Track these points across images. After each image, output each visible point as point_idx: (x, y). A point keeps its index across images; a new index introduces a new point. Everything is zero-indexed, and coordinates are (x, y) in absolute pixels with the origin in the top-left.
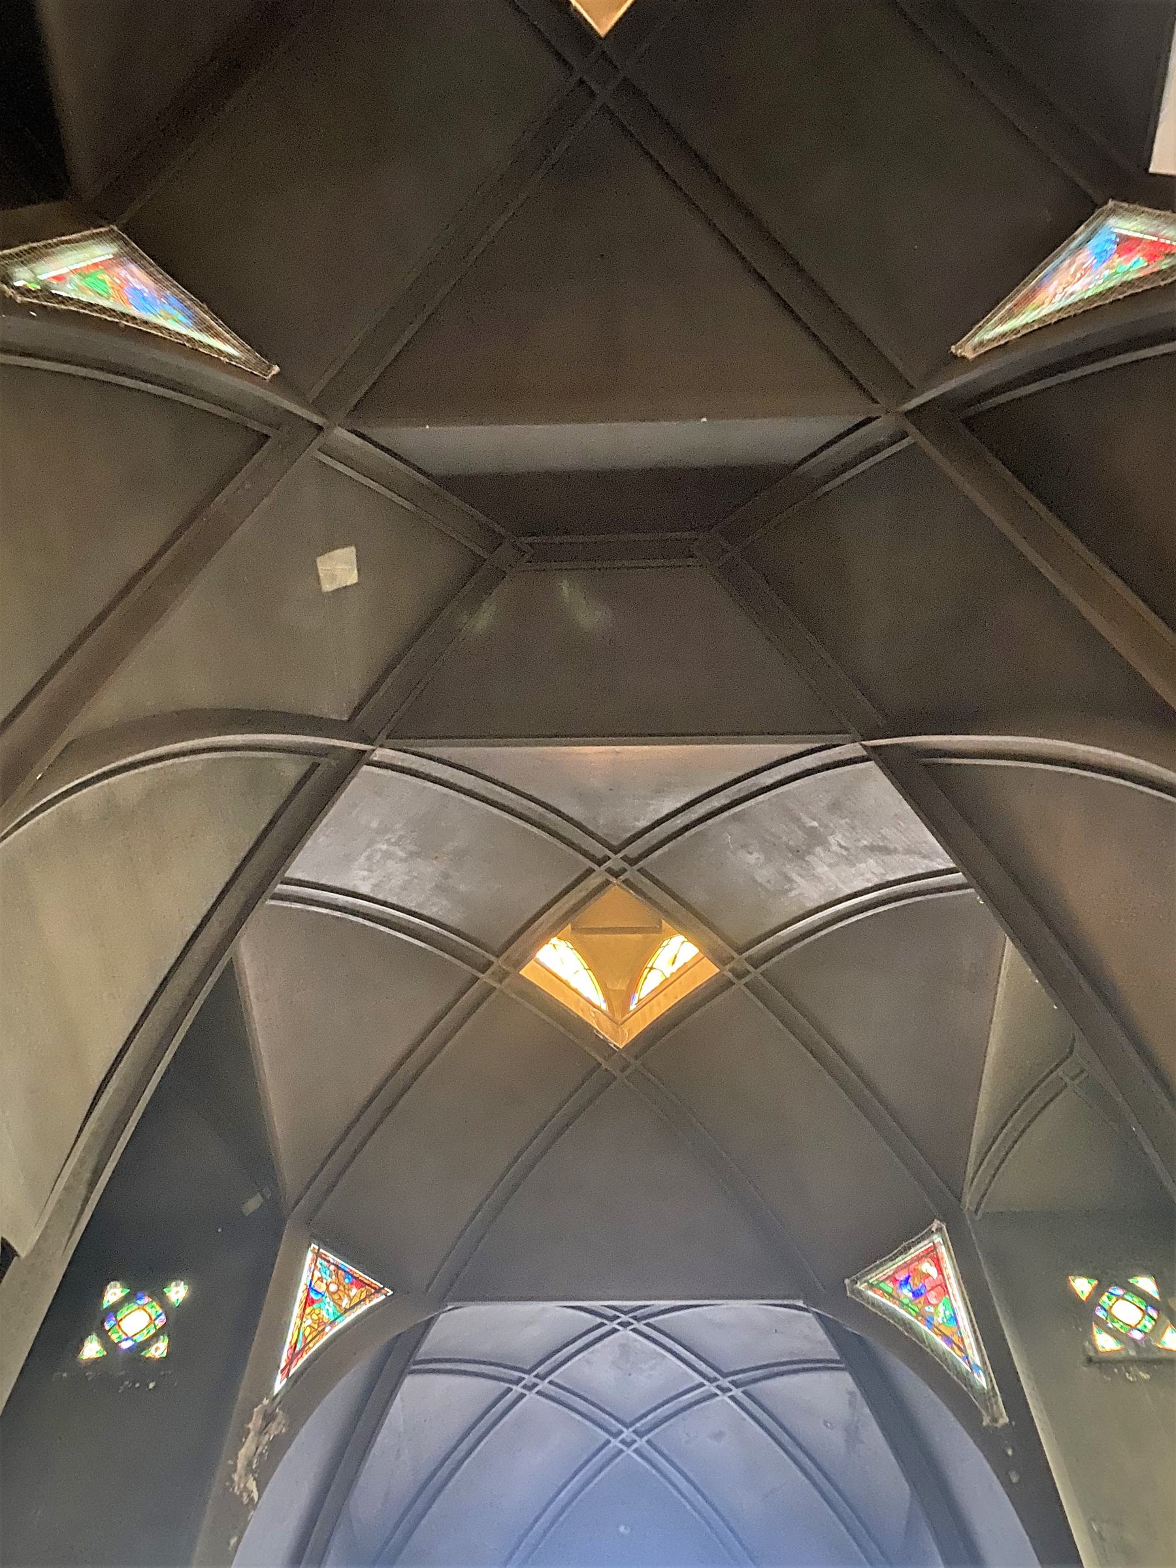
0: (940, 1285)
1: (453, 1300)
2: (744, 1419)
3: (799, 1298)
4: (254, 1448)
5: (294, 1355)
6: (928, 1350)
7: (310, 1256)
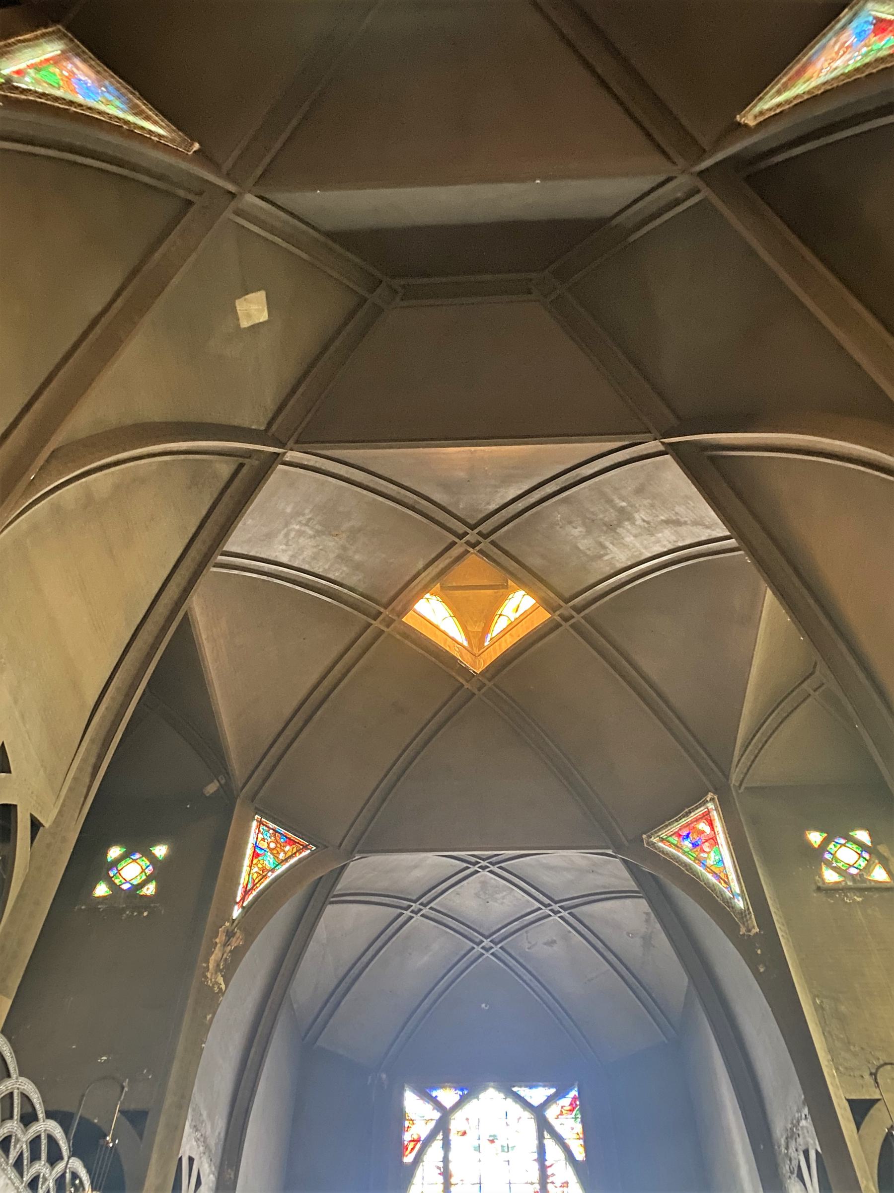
0: (712, 839)
1: (359, 852)
2: (570, 932)
3: (609, 848)
4: (220, 955)
5: (246, 893)
6: (702, 883)
7: (254, 824)
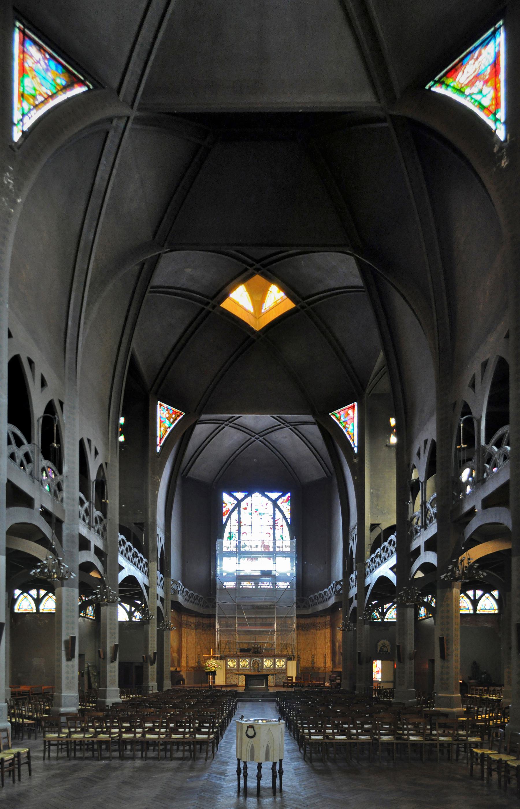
5: (161, 439)
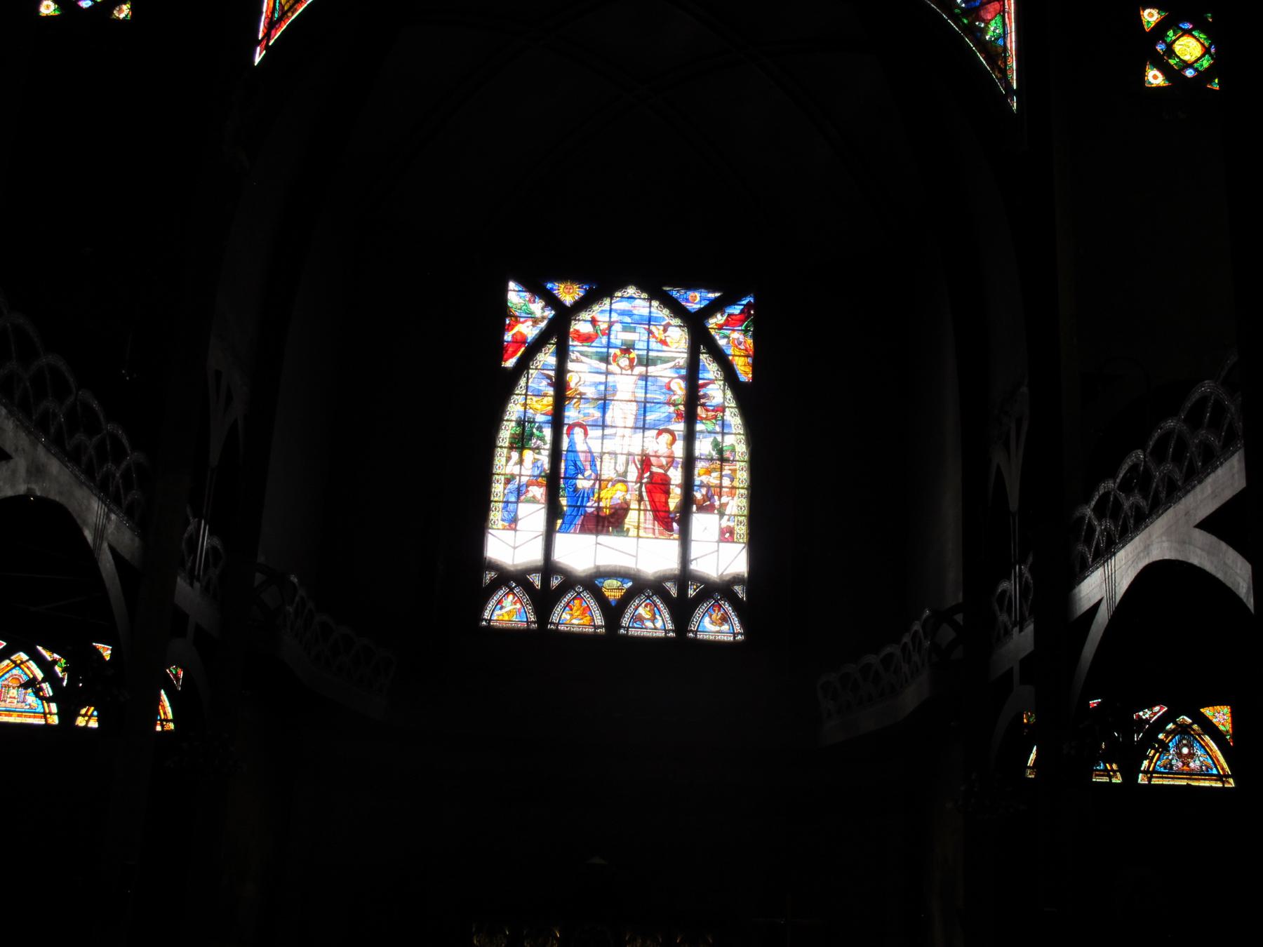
5: (272, 25)
